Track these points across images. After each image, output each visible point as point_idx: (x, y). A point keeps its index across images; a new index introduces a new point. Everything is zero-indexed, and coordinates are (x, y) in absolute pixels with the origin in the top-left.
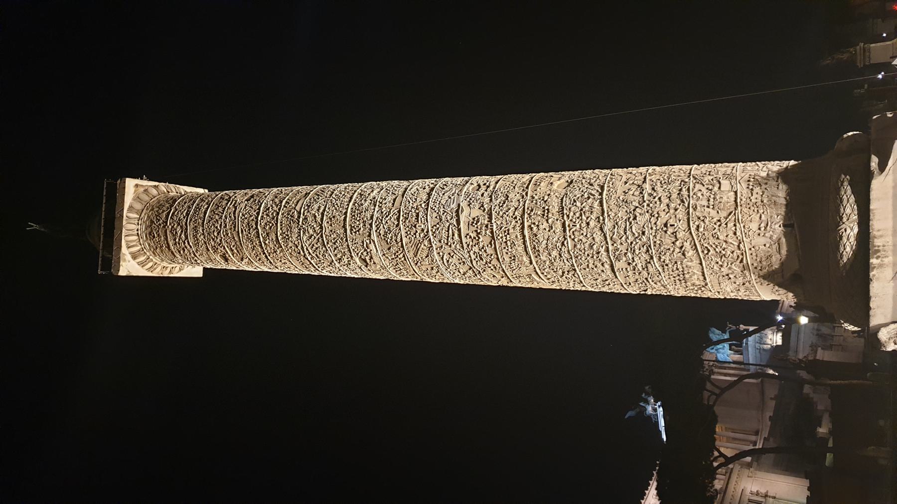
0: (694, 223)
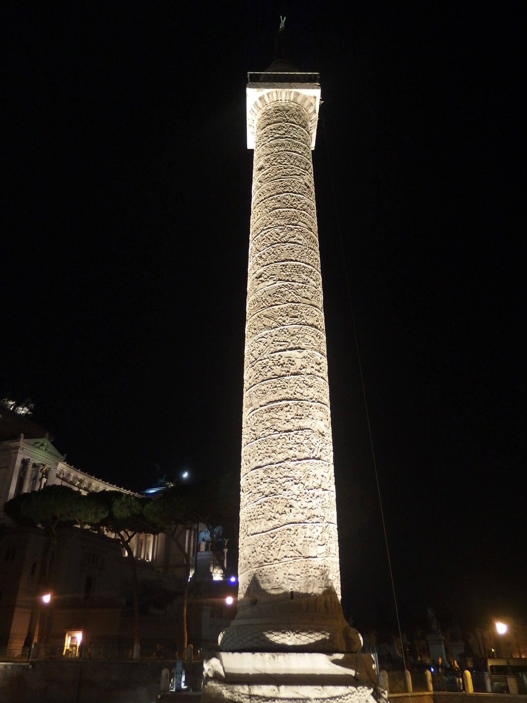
0: (292, 527)
